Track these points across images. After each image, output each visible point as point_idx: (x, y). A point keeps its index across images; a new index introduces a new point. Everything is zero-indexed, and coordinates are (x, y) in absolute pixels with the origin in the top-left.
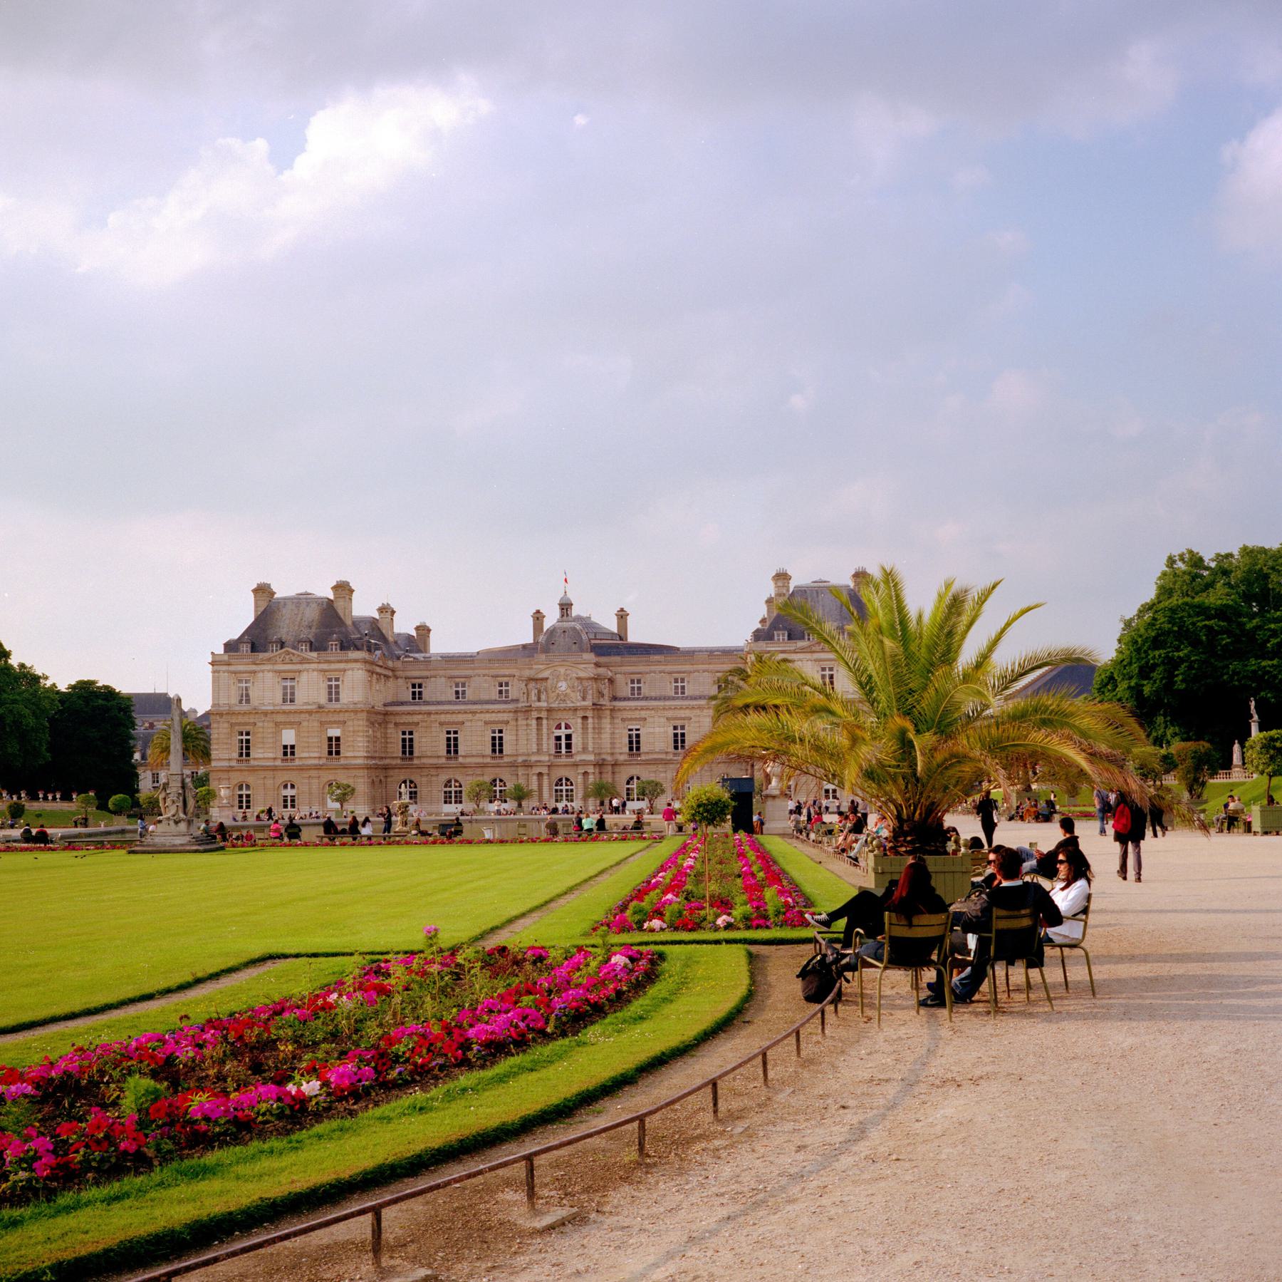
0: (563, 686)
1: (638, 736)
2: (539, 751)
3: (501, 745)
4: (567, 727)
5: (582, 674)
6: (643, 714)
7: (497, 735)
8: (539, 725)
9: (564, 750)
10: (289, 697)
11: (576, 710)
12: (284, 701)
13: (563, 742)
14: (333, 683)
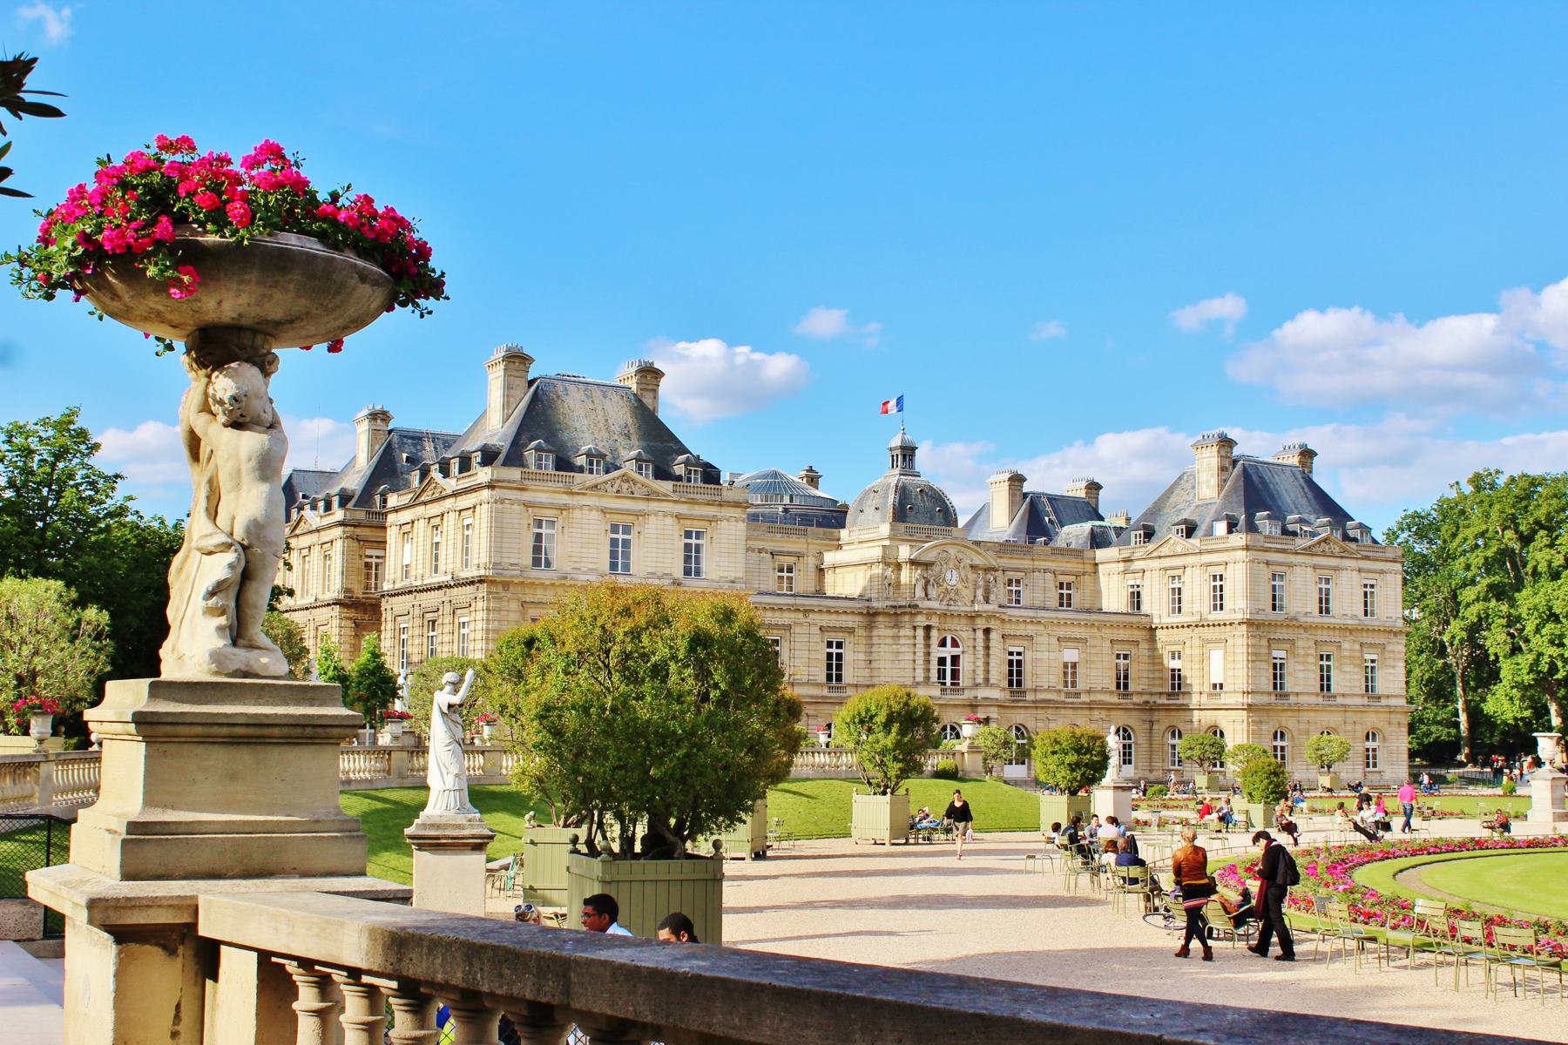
0: (952, 578)
1: (1019, 662)
2: (927, 678)
3: (839, 667)
4: (955, 644)
5: (978, 561)
6: (1030, 629)
7: (834, 650)
8: (927, 637)
9: (948, 680)
10: (619, 555)
11: (972, 617)
12: (613, 566)
13: (948, 668)
14: (693, 541)
